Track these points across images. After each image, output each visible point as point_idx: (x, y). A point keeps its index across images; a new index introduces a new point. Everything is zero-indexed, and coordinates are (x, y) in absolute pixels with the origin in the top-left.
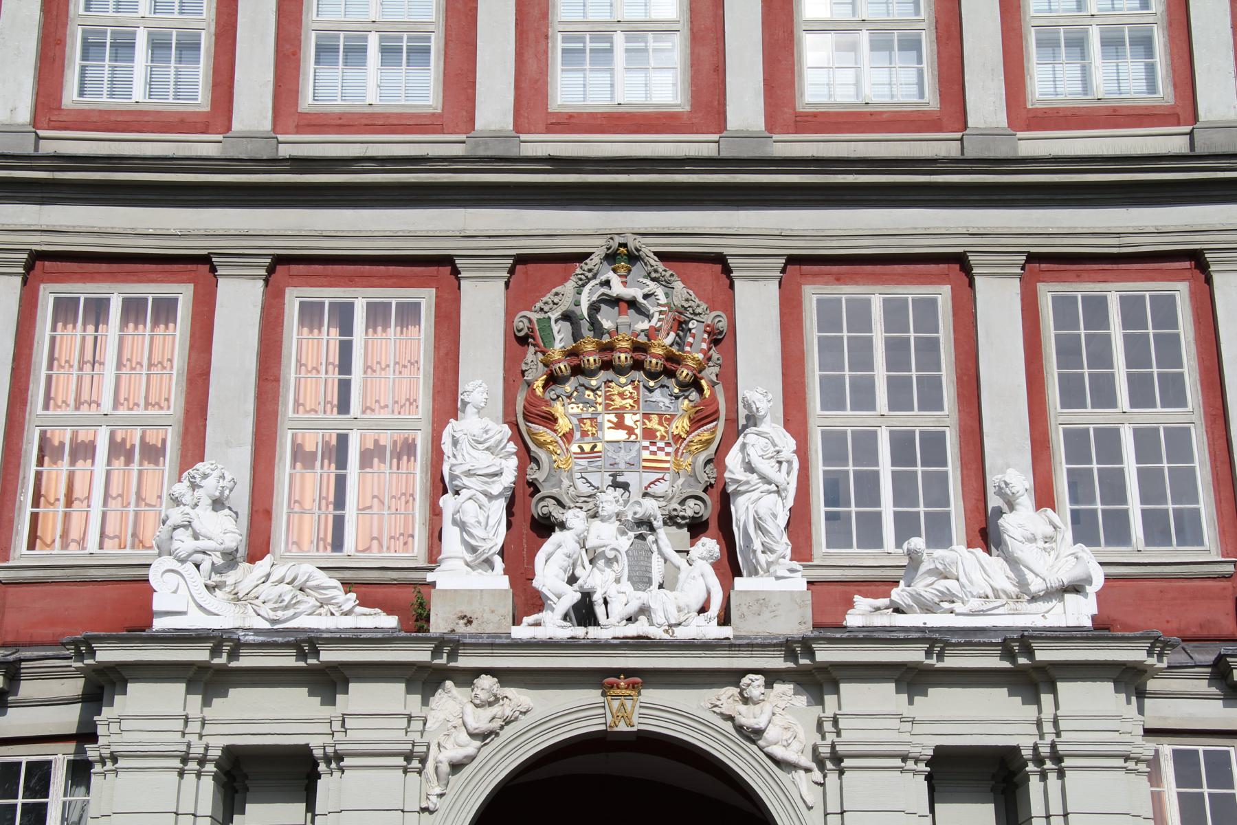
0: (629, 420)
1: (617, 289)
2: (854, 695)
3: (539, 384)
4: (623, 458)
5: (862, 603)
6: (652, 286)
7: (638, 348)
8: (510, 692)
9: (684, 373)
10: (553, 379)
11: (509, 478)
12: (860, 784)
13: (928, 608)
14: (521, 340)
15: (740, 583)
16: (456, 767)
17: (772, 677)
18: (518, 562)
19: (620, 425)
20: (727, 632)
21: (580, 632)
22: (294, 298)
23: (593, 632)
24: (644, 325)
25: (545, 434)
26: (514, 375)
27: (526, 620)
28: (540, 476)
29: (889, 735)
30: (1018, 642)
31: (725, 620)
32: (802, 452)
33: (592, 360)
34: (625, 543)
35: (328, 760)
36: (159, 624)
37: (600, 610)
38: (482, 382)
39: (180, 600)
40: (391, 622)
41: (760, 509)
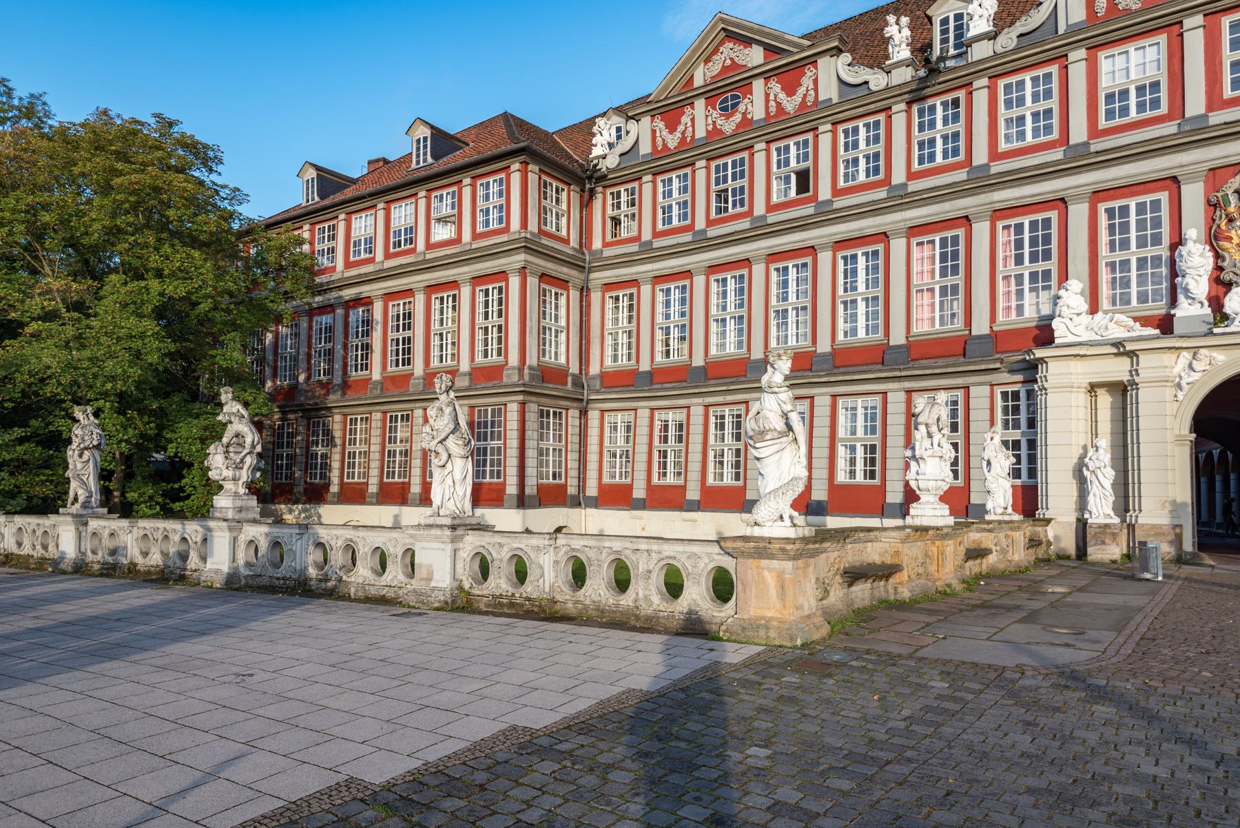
14: (1213, 206)
18: (1216, 304)
25: (1226, 244)
28: (1225, 264)
36: (1057, 341)
38: (1193, 232)
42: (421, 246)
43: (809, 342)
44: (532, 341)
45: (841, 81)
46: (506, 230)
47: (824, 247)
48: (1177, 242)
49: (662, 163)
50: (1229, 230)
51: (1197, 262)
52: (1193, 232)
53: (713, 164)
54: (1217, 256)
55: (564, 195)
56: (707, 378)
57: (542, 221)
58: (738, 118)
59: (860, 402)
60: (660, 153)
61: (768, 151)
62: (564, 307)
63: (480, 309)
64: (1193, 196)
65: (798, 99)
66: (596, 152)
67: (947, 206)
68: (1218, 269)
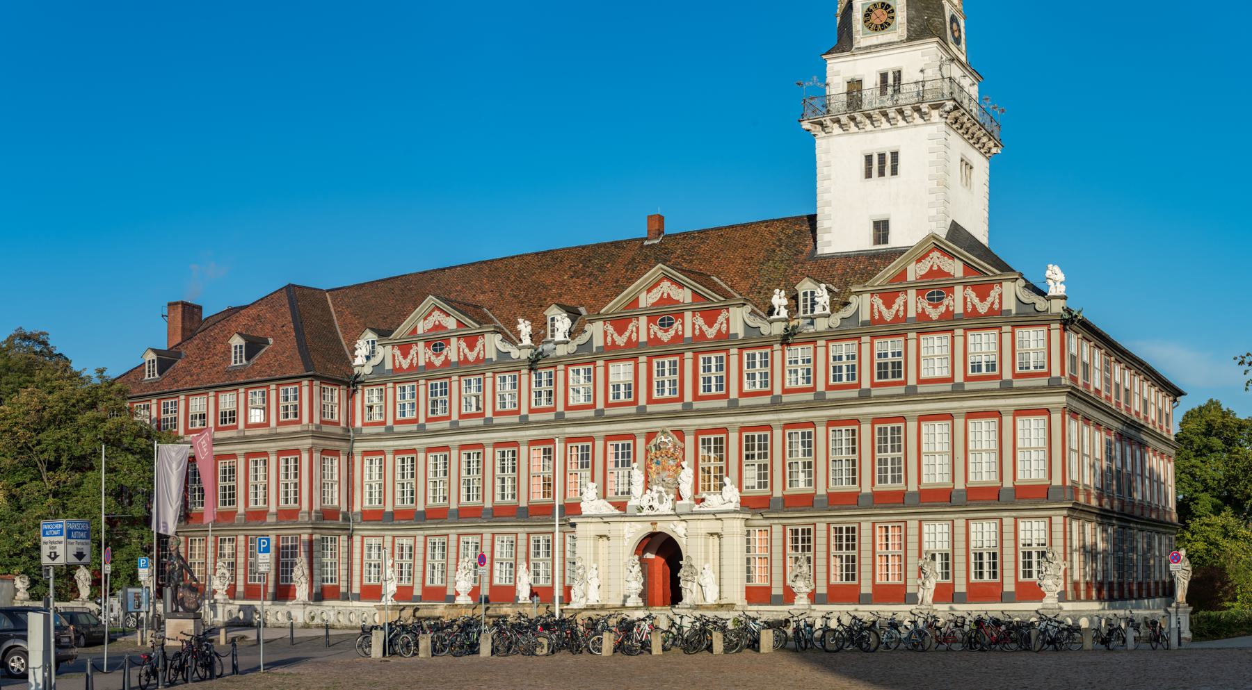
14: (647, 451)
22: (609, 443)
39: (586, 508)
42: (241, 425)
43: (480, 501)
44: (316, 495)
45: (498, 350)
46: (300, 422)
47: (488, 445)
49: (399, 376)
53: (429, 383)
55: (336, 392)
56: (426, 519)
57: (323, 414)
58: (442, 358)
59: (505, 538)
60: (397, 370)
61: (460, 381)
62: (336, 467)
63: (282, 471)
64: (641, 442)
65: (475, 353)
66: (358, 361)
67: (545, 431)
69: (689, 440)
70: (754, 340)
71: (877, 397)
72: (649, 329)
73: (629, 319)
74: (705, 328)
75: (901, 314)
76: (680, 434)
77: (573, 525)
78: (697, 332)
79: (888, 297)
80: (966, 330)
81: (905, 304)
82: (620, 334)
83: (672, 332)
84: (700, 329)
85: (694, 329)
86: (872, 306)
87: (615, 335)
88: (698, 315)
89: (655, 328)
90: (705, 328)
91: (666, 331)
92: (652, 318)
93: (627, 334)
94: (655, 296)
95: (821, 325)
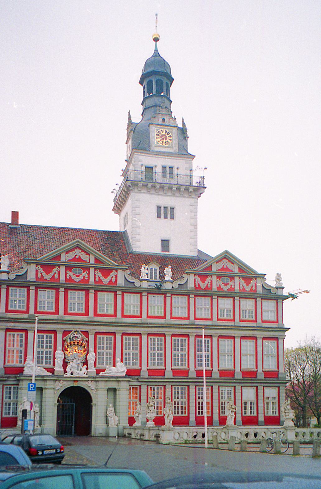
0: (76, 351)
1: (76, 335)
2: (100, 383)
3: (66, 347)
4: (76, 355)
5: (101, 373)
6: (80, 335)
7: (78, 343)
8: (64, 382)
9: (83, 346)
10: (68, 346)
11: (63, 358)
12: (99, 392)
13: (108, 374)
15: (88, 370)
16: (58, 389)
17: (92, 381)
19: (75, 351)
20: (87, 376)
21: (72, 376)
23: (73, 376)
24: (78, 340)
25: (67, 352)
26: (63, 345)
27: (66, 374)
29: (103, 387)
30: (117, 377)
31: (87, 374)
32: (96, 355)
33: (73, 344)
34: (76, 366)
35: (44, 388)
37: (73, 373)
40: (51, 374)
41: (91, 362)
48: (55, 350)
50: (68, 348)
51: (60, 354)
52: (59, 347)
54: (65, 355)
64: (60, 336)
68: (65, 358)
69: (91, 337)
70: (130, 289)
71: (198, 325)
72: (66, 274)
73: (53, 266)
74: (102, 278)
75: (209, 286)
76: (86, 333)
77: (19, 380)
78: (97, 279)
79: (203, 277)
80: (240, 298)
81: (211, 281)
82: (47, 273)
83: (81, 277)
84: (99, 278)
85: (95, 278)
86: (195, 280)
87: (44, 274)
88: (98, 271)
89: (69, 274)
90: (102, 278)
91: (78, 276)
92: (69, 268)
93: (52, 274)
94: (71, 255)
95: (168, 286)
